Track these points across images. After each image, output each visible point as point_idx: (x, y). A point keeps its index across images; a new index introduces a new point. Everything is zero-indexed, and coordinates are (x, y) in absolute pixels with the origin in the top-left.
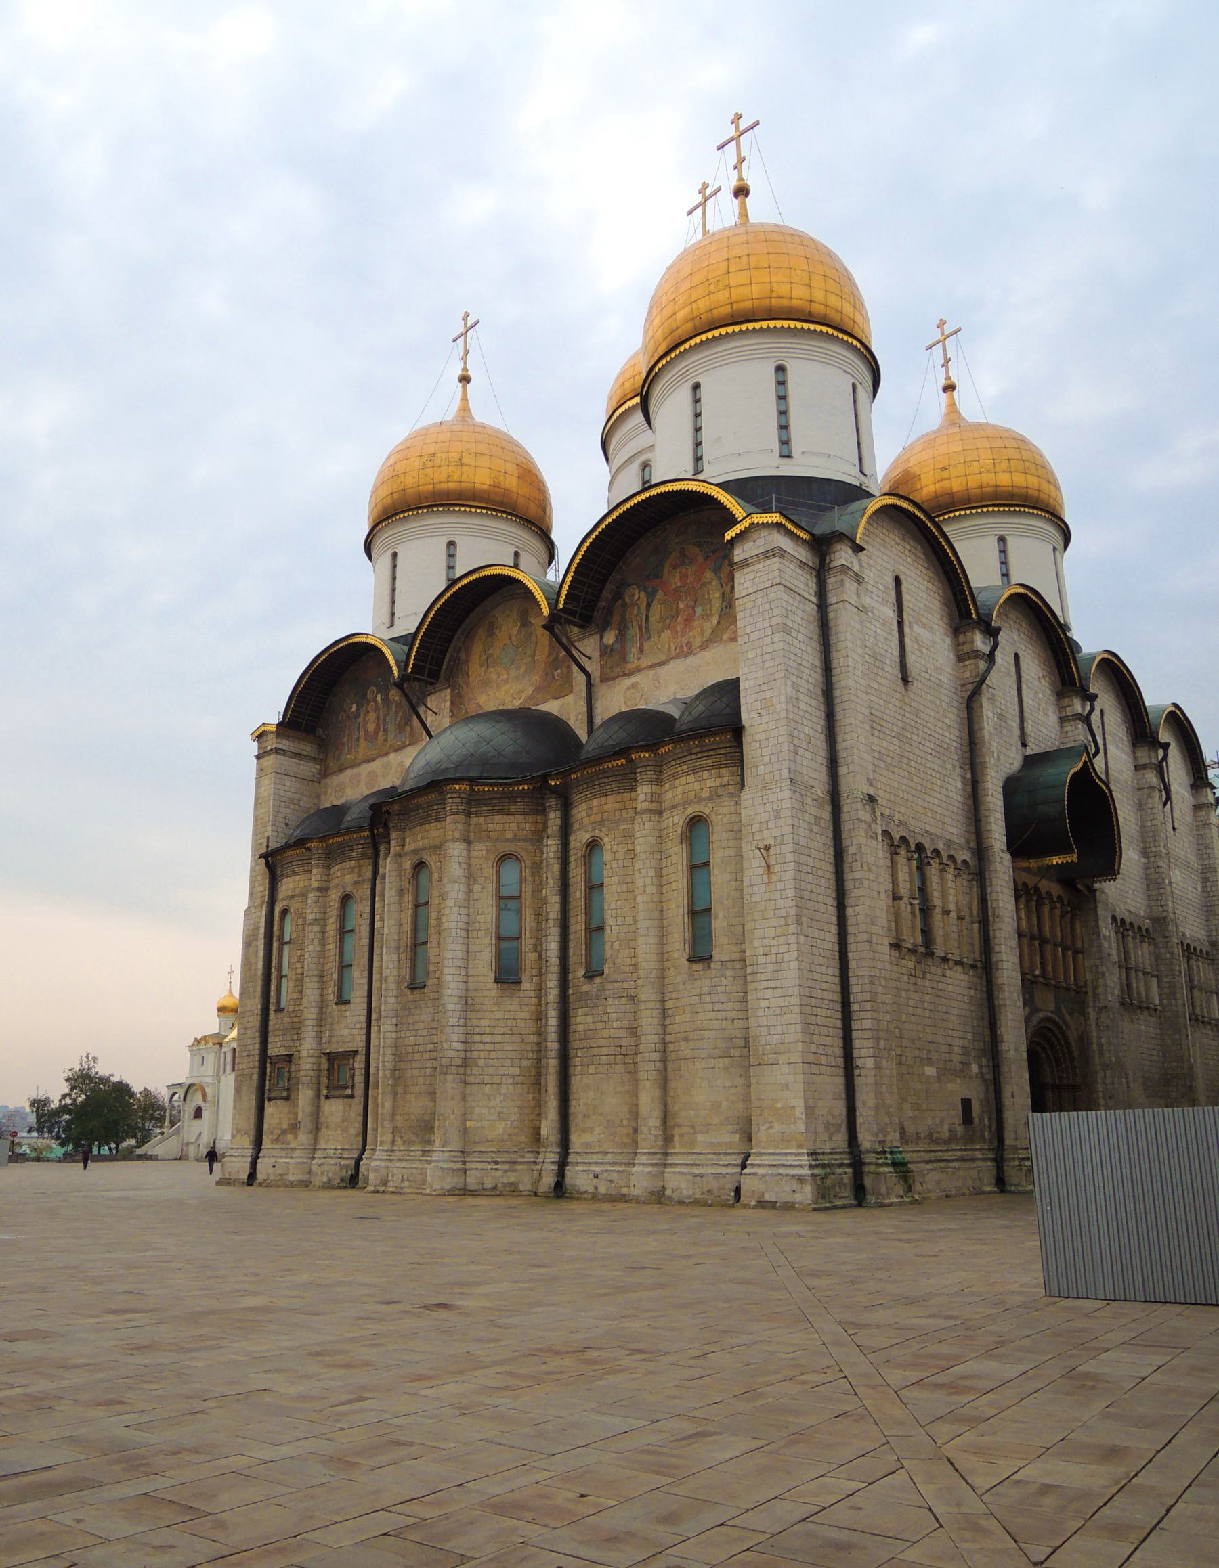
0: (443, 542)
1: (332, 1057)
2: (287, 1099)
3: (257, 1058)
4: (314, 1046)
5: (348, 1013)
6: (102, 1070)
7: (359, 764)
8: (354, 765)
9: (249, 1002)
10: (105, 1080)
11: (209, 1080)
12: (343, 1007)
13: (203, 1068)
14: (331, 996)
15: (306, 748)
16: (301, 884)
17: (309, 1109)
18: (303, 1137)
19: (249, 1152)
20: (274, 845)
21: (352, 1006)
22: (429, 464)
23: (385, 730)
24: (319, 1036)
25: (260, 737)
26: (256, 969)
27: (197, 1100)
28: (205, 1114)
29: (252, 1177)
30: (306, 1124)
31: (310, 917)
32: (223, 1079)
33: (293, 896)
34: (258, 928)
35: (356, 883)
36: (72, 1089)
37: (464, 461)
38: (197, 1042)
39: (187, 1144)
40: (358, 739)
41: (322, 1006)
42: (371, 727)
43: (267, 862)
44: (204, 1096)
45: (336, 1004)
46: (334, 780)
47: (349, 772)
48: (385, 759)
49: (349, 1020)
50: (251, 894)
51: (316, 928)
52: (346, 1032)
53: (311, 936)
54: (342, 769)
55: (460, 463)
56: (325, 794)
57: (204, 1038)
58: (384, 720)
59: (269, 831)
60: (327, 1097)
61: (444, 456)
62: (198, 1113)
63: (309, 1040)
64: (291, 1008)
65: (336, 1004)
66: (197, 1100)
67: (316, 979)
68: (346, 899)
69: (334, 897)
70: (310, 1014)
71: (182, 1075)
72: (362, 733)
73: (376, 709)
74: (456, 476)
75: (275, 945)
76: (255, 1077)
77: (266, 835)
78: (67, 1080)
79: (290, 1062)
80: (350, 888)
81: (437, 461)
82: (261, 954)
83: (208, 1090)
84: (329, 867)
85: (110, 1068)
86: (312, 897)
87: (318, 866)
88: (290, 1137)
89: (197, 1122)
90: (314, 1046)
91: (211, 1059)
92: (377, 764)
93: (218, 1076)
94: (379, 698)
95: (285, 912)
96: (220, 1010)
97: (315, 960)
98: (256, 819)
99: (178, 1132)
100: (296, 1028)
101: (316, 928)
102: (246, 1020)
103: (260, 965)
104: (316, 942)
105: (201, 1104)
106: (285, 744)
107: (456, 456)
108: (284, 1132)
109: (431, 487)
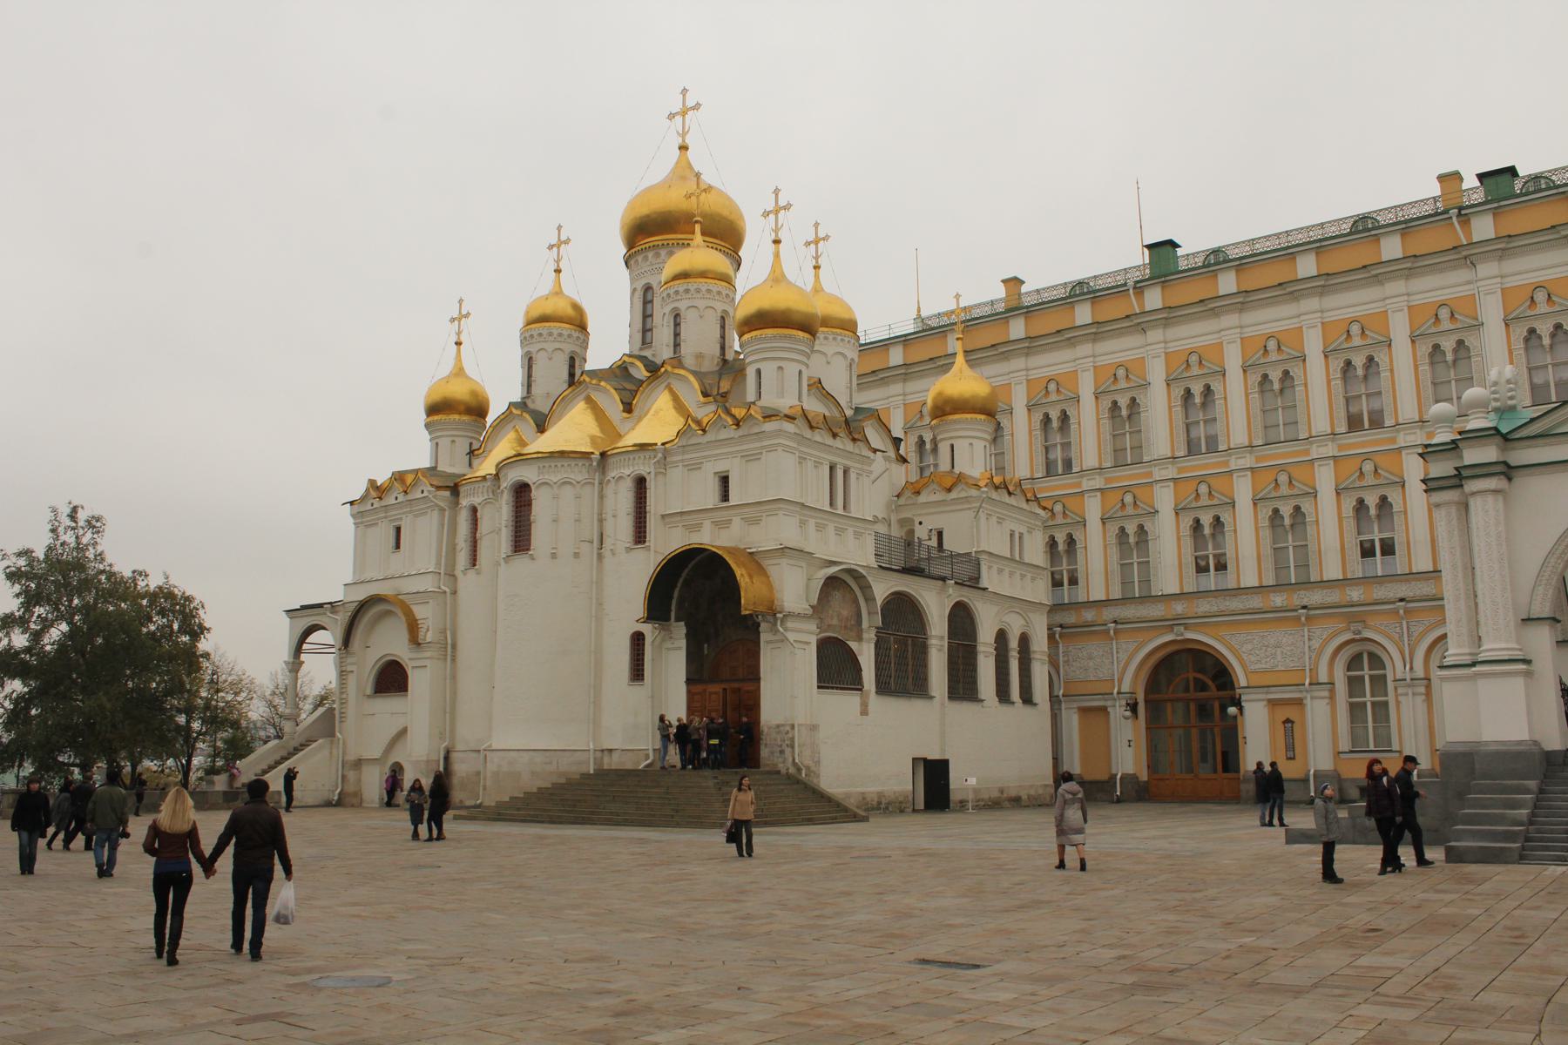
10: (120, 588)
11: (427, 584)
13: (397, 564)
28: (416, 680)
32: (468, 583)
36: (31, 599)
38: (377, 490)
39: (358, 763)
44: (413, 627)
62: (391, 679)
66: (389, 642)
71: (333, 583)
78: (13, 576)
83: (420, 612)
89: (389, 704)
91: (424, 533)
93: (452, 576)
96: (433, 409)
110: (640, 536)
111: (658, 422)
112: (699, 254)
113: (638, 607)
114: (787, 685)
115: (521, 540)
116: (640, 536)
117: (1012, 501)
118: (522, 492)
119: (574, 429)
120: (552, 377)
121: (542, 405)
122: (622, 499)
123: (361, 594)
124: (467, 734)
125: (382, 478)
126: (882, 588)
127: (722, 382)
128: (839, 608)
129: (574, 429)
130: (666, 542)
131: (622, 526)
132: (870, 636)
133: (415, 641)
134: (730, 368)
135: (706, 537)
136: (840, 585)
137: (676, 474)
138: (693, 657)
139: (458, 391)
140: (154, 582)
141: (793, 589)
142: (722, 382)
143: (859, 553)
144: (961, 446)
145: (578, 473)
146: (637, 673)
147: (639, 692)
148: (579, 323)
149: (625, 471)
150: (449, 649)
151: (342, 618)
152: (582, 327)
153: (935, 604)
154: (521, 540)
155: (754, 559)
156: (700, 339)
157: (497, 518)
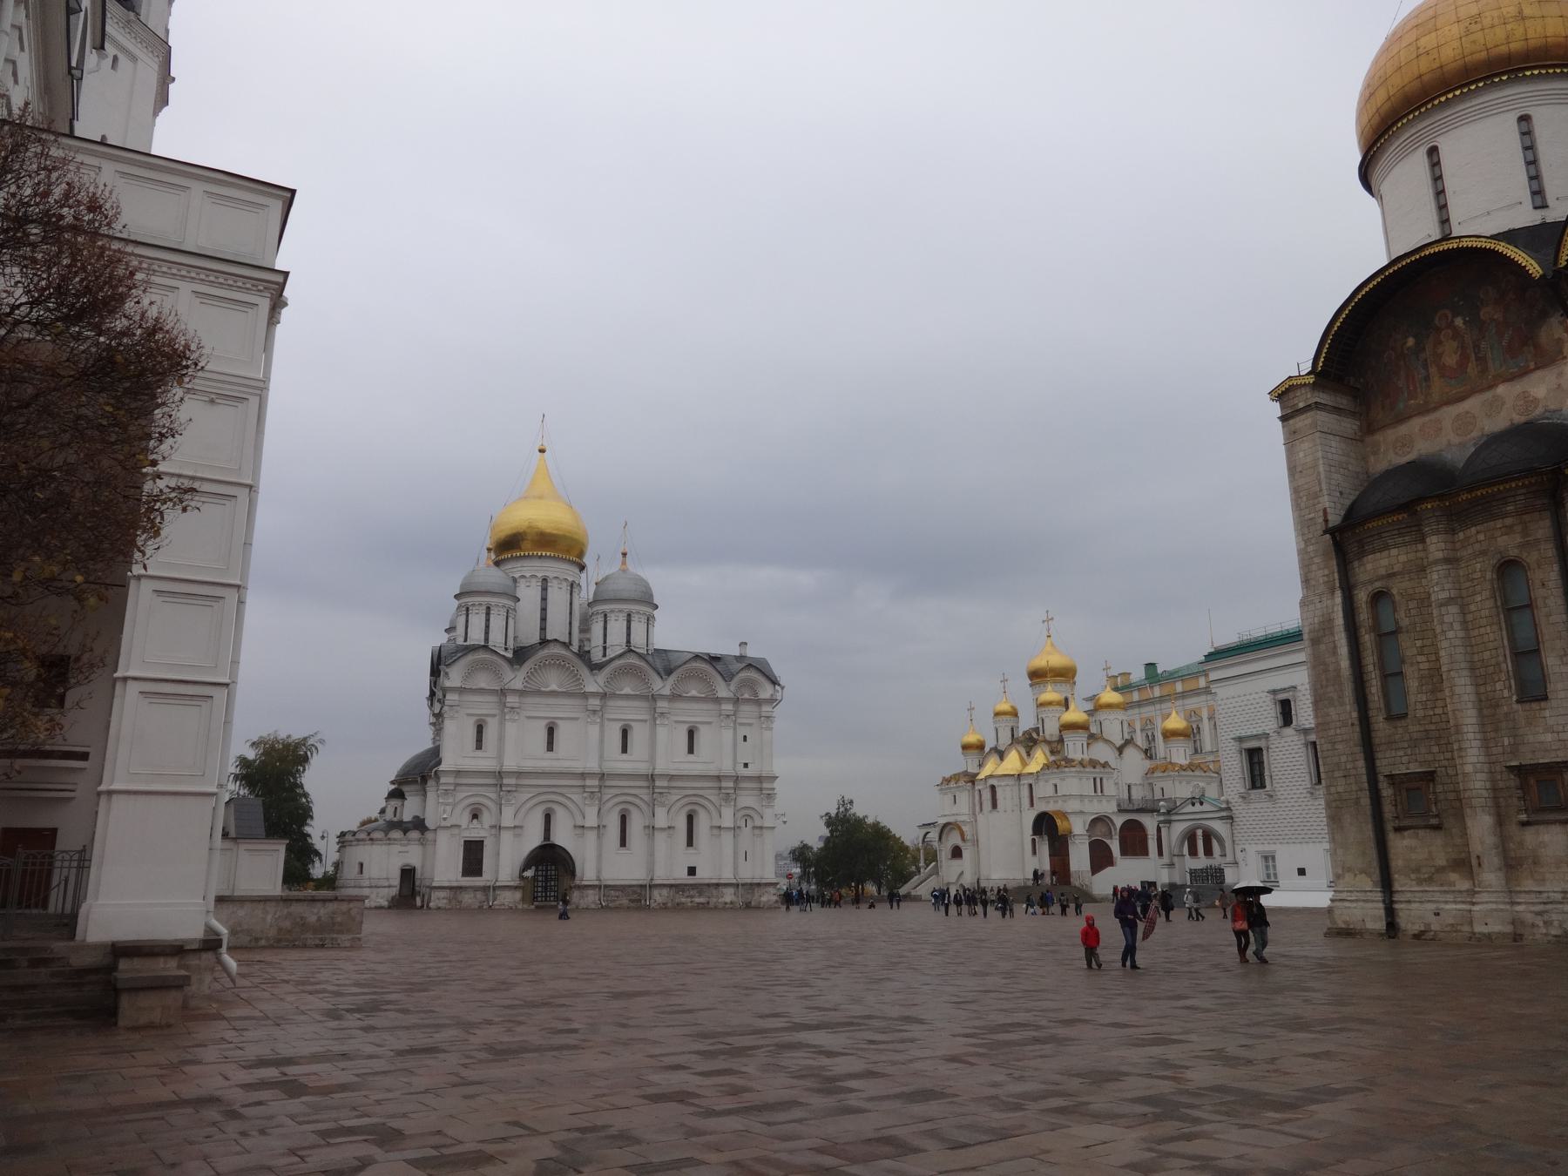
0: (1512, 118)
1: (1521, 771)
2: (1437, 828)
3: (1365, 778)
4: (1482, 759)
5: (1547, 713)
6: (858, 810)
7: (1435, 409)
8: (1425, 410)
9: (1333, 713)
10: (859, 822)
12: (1535, 706)
14: (1504, 689)
15: (1343, 401)
16: (1403, 558)
17: (1490, 840)
18: (1491, 877)
19: (1379, 896)
20: (1335, 519)
21: (1554, 703)
22: (1474, 27)
23: (1481, 360)
24: (1486, 745)
25: (1283, 394)
26: (1338, 670)
27: (954, 839)
29: (1392, 927)
30: (1492, 860)
31: (1439, 594)
32: (980, 818)
33: (1391, 576)
34: (1331, 621)
35: (1522, 546)
37: (1527, 11)
38: (947, 781)
40: (1427, 378)
41: (1488, 708)
42: (1451, 360)
43: (1334, 538)
44: (962, 834)
45: (1518, 702)
46: (1391, 435)
47: (1416, 424)
48: (1488, 395)
49: (1551, 722)
50: (1306, 581)
51: (1453, 609)
52: (1549, 737)
53: (1447, 619)
54: (1401, 419)
55: (1520, 17)
56: (1375, 453)
57: (956, 778)
58: (1476, 347)
59: (1325, 501)
60: (1524, 824)
61: (1496, 13)
62: (957, 853)
63: (1475, 751)
64: (1420, 713)
65: (1518, 702)
66: (954, 839)
67: (1465, 673)
68: (1507, 568)
69: (1483, 569)
70: (1469, 719)
72: (1433, 370)
73: (1456, 335)
74: (1519, 33)
75: (1367, 639)
76: (1366, 801)
77: (1320, 507)
79: (1433, 780)
80: (1513, 553)
81: (1487, 22)
82: (1344, 650)
84: (1453, 532)
85: (868, 809)
86: (1435, 575)
87: (1437, 532)
88: (1453, 876)
89: (956, 862)
90: (1482, 759)
91: (964, 798)
92: (1472, 404)
94: (1459, 322)
95: (1378, 597)
97: (1461, 650)
98: (1296, 491)
99: (936, 871)
100: (1442, 735)
101: (1453, 609)
102: (1332, 732)
103: (1345, 664)
104: (1457, 626)
105: (959, 842)
106: (1323, 398)
107: (1512, 10)
108: (1441, 870)
109: (1484, 54)
110: (1032, 804)
111: (1040, 758)
112: (1050, 694)
113: (1030, 831)
114: (1079, 858)
115: (994, 806)
116: (1032, 804)
117: (1197, 773)
118: (993, 788)
119: (1012, 763)
120: (1005, 739)
121: (1002, 748)
122: (1025, 792)
123: (942, 821)
124: (984, 873)
125: (947, 776)
126: (1119, 821)
127: (1056, 746)
128: (1100, 828)
129: (1012, 763)
130: (1041, 807)
131: (1026, 801)
132: (1116, 837)
133: (963, 839)
134: (1061, 740)
135: (1049, 807)
136: (1099, 821)
137: (1041, 783)
138: (1051, 846)
139: (972, 738)
140: (870, 821)
141: (1078, 827)
142: (1056, 746)
143: (1109, 808)
144: (1174, 750)
145: (1011, 782)
146: (1034, 852)
147: (1036, 859)
148: (1014, 713)
149: (1025, 782)
150: (976, 842)
151: (938, 829)
152: (1016, 715)
153: (1150, 823)
154: (994, 806)
155: (1064, 815)
156: (1051, 730)
157: (987, 795)
